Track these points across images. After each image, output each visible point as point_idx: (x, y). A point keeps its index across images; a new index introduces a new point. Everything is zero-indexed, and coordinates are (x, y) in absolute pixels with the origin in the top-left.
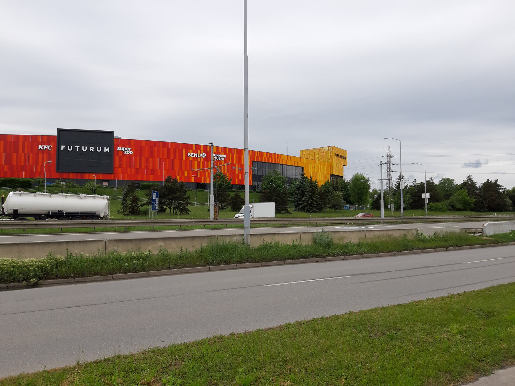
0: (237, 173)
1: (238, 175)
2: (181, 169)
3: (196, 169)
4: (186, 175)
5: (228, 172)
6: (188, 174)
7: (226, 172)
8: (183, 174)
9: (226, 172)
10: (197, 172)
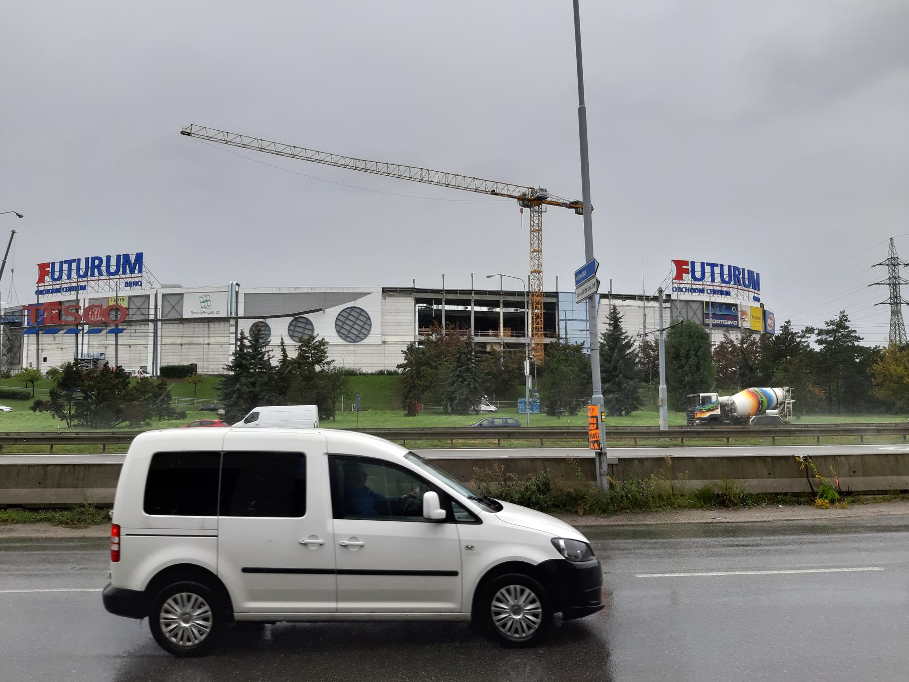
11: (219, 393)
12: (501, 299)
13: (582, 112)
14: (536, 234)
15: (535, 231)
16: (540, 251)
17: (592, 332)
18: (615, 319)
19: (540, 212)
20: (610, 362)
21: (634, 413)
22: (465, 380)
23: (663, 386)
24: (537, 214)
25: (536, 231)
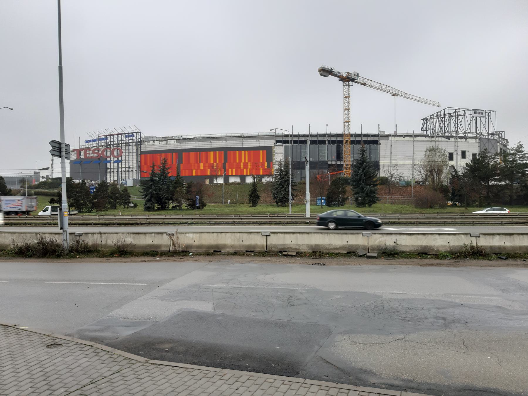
0: (261, 161)
1: (263, 163)
2: (197, 162)
3: (212, 161)
4: (202, 168)
5: (249, 161)
6: (204, 167)
7: (247, 161)
8: (199, 167)
9: (247, 161)
10: (213, 164)
11: (142, 194)
12: (327, 139)
13: (60, 68)
14: (347, 99)
15: (346, 97)
16: (349, 109)
17: (64, 175)
18: (363, 151)
19: (349, 86)
20: (357, 175)
21: (373, 205)
22: (283, 187)
23: (308, 193)
24: (347, 87)
25: (347, 97)
